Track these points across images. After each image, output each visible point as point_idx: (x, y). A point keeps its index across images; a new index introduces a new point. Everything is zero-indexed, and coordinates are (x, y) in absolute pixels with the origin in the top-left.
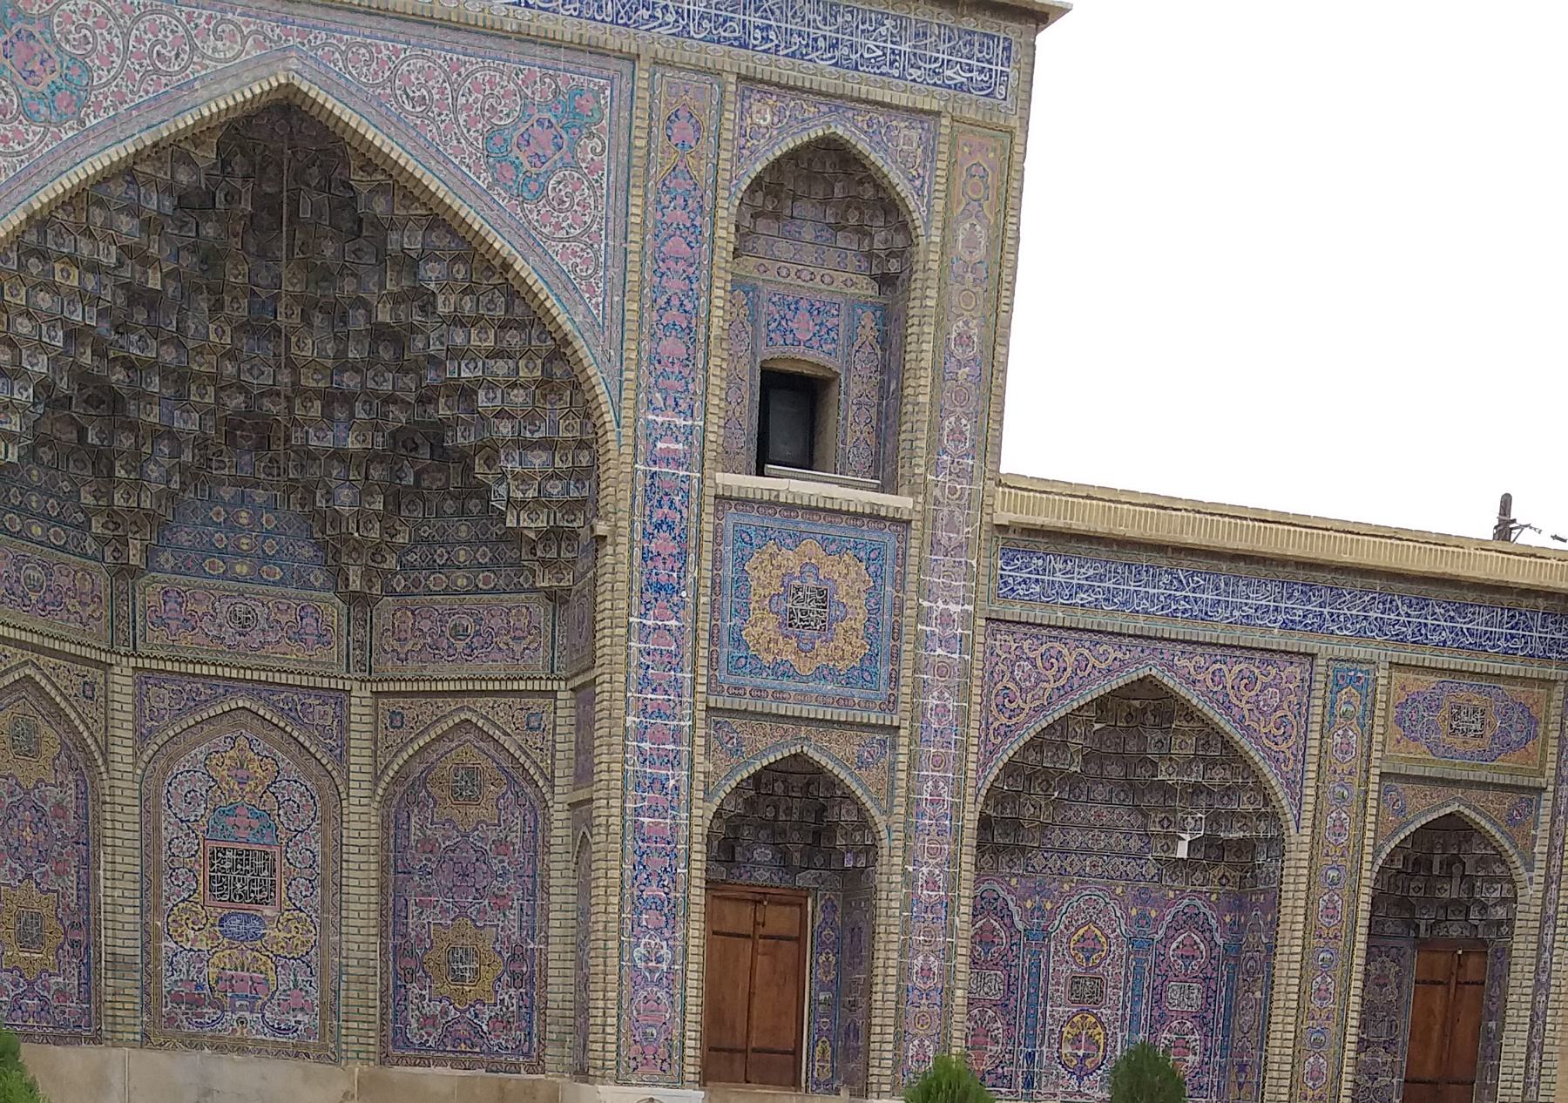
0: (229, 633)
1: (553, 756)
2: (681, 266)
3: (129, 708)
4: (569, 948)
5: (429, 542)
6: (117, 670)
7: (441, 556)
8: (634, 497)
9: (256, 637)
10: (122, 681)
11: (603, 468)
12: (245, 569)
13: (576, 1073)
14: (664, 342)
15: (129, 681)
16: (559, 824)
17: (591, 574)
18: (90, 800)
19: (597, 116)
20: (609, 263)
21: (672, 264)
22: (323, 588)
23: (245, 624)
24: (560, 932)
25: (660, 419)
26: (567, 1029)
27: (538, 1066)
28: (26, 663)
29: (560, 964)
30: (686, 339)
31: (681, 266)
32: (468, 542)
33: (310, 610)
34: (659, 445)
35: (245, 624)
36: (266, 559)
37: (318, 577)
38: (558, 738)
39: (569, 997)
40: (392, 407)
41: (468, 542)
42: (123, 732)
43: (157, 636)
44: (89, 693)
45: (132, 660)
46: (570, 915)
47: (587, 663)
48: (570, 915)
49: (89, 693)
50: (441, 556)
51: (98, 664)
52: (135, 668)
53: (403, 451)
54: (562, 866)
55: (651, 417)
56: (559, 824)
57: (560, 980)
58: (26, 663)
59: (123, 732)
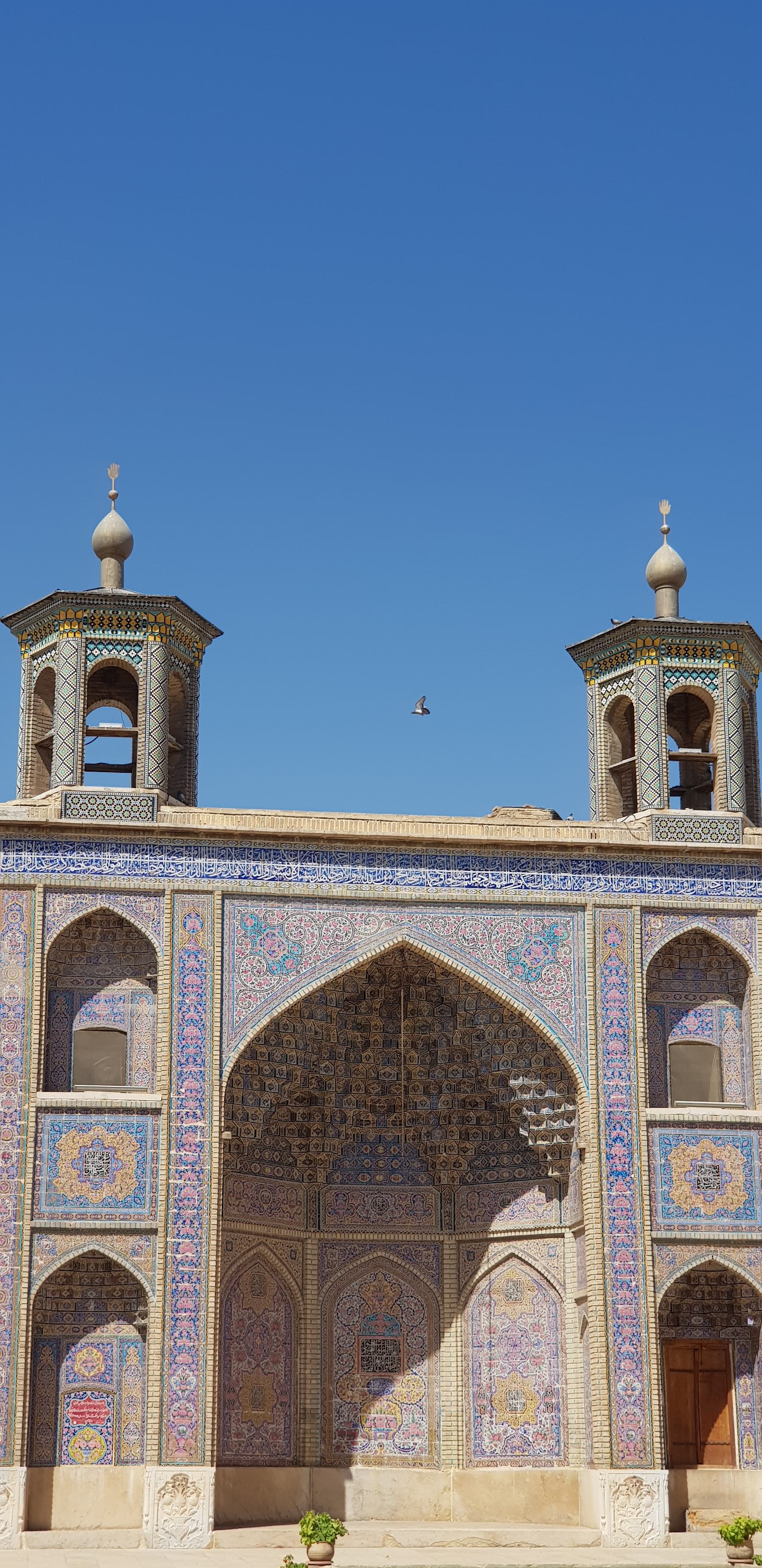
0: (373, 1215)
1: (564, 1271)
2: (617, 1004)
3: (315, 1262)
4: (580, 1385)
5: (486, 1153)
6: (309, 1241)
7: (493, 1161)
8: (599, 1126)
9: (388, 1215)
10: (312, 1248)
11: (581, 1111)
12: (381, 1178)
13: (588, 1463)
14: (611, 1043)
15: (316, 1247)
16: (570, 1311)
17: (578, 1168)
18: (295, 1318)
19: (566, 935)
20: (578, 1006)
21: (612, 1004)
22: (426, 1184)
23: (382, 1208)
24: (574, 1376)
25: (611, 1084)
26: (581, 1436)
27: (565, 1462)
28: (260, 1243)
29: (575, 1396)
30: (623, 1040)
31: (617, 1004)
32: (509, 1153)
33: (418, 1197)
34: (612, 1097)
35: (382, 1208)
36: (393, 1171)
37: (423, 1178)
38: (566, 1261)
39: (581, 1416)
40: (462, 1086)
41: (509, 1153)
42: (312, 1276)
43: (331, 1220)
44: (293, 1256)
45: (318, 1235)
46: (579, 1365)
47: (579, 1218)
48: (579, 1365)
49: (293, 1256)
50: (493, 1161)
51: (298, 1240)
52: (319, 1240)
53: (470, 1107)
54: (573, 1336)
55: (606, 1083)
56: (570, 1311)
57: (575, 1406)
58: (260, 1243)
59: (312, 1276)
